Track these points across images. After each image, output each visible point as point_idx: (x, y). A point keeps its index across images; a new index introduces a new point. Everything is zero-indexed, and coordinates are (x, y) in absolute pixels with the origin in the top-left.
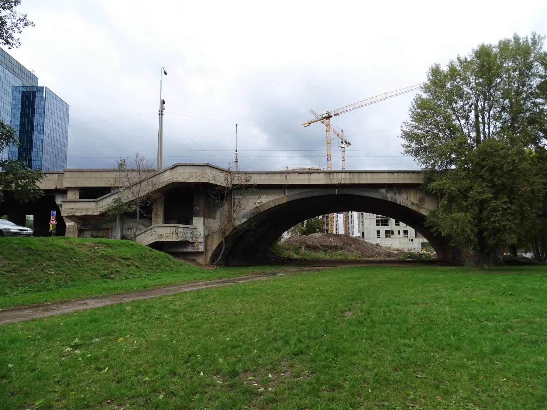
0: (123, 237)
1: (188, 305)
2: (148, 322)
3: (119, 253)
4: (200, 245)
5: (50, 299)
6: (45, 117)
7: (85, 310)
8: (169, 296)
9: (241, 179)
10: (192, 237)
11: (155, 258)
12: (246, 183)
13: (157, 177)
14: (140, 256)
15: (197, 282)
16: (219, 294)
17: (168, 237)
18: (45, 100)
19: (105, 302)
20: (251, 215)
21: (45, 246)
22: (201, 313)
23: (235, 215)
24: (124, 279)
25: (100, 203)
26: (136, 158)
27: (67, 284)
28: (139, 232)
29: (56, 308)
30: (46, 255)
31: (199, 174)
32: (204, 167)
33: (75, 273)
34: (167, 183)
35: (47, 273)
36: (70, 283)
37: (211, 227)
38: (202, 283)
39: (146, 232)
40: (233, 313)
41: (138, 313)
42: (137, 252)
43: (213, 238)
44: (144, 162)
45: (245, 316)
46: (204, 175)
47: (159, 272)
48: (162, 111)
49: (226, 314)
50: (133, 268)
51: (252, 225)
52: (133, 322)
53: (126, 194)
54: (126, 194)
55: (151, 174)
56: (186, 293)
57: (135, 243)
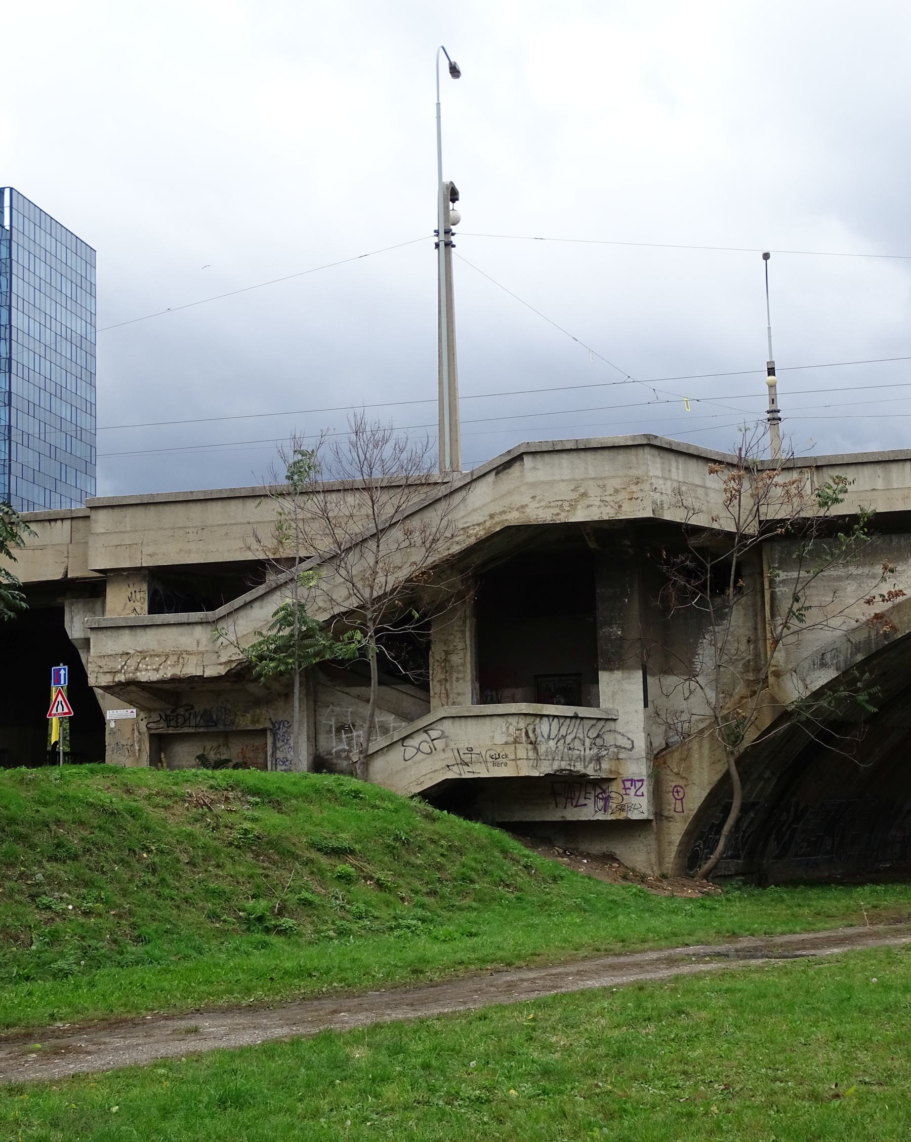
0: (320, 764)
1: (602, 1050)
2: (444, 1113)
3: (308, 827)
4: (632, 792)
5: (65, 1010)
6: (14, 304)
7: (198, 1057)
8: (520, 1007)
9: (800, 495)
10: (598, 759)
11: (450, 848)
12: (822, 513)
13: (441, 507)
14: (390, 841)
15: (633, 952)
16: (734, 1006)
17: (496, 759)
18: (11, 240)
19: (265, 1028)
20: (853, 654)
21: (39, 802)
22: (659, 1084)
23: (779, 657)
24: (331, 933)
25: (227, 626)
26: (353, 436)
27: (121, 953)
28: (380, 742)
29: (91, 1048)
30: (42, 839)
31: (617, 483)
32: (633, 451)
33: (147, 911)
34: (481, 533)
35: (48, 908)
36: (134, 950)
37: (678, 713)
38: (654, 955)
39: (409, 742)
40: (804, 1089)
41: (400, 1074)
42: (377, 824)
43: (686, 758)
44: (388, 451)
45: (860, 1105)
46: (634, 488)
47: (471, 908)
48: (448, 232)
49: (773, 1093)
50: (364, 890)
51: (862, 697)
52: (383, 1113)
53: (324, 586)
54: (324, 586)
55: (416, 499)
56: (590, 996)
57: (368, 785)
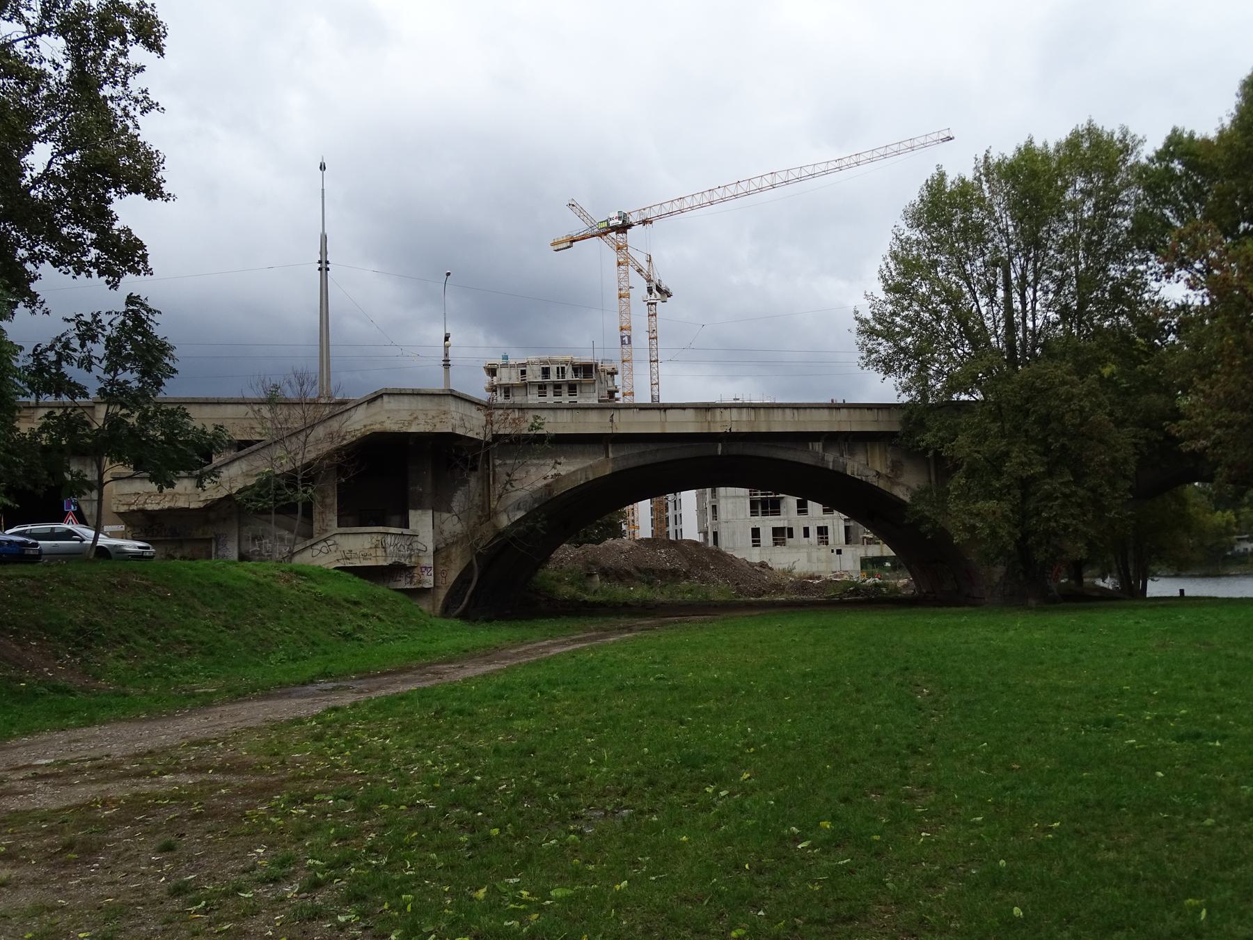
10: (410, 556)
39: (316, 547)
